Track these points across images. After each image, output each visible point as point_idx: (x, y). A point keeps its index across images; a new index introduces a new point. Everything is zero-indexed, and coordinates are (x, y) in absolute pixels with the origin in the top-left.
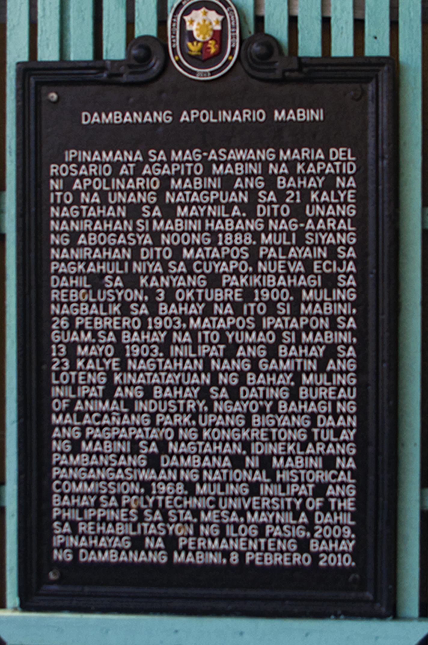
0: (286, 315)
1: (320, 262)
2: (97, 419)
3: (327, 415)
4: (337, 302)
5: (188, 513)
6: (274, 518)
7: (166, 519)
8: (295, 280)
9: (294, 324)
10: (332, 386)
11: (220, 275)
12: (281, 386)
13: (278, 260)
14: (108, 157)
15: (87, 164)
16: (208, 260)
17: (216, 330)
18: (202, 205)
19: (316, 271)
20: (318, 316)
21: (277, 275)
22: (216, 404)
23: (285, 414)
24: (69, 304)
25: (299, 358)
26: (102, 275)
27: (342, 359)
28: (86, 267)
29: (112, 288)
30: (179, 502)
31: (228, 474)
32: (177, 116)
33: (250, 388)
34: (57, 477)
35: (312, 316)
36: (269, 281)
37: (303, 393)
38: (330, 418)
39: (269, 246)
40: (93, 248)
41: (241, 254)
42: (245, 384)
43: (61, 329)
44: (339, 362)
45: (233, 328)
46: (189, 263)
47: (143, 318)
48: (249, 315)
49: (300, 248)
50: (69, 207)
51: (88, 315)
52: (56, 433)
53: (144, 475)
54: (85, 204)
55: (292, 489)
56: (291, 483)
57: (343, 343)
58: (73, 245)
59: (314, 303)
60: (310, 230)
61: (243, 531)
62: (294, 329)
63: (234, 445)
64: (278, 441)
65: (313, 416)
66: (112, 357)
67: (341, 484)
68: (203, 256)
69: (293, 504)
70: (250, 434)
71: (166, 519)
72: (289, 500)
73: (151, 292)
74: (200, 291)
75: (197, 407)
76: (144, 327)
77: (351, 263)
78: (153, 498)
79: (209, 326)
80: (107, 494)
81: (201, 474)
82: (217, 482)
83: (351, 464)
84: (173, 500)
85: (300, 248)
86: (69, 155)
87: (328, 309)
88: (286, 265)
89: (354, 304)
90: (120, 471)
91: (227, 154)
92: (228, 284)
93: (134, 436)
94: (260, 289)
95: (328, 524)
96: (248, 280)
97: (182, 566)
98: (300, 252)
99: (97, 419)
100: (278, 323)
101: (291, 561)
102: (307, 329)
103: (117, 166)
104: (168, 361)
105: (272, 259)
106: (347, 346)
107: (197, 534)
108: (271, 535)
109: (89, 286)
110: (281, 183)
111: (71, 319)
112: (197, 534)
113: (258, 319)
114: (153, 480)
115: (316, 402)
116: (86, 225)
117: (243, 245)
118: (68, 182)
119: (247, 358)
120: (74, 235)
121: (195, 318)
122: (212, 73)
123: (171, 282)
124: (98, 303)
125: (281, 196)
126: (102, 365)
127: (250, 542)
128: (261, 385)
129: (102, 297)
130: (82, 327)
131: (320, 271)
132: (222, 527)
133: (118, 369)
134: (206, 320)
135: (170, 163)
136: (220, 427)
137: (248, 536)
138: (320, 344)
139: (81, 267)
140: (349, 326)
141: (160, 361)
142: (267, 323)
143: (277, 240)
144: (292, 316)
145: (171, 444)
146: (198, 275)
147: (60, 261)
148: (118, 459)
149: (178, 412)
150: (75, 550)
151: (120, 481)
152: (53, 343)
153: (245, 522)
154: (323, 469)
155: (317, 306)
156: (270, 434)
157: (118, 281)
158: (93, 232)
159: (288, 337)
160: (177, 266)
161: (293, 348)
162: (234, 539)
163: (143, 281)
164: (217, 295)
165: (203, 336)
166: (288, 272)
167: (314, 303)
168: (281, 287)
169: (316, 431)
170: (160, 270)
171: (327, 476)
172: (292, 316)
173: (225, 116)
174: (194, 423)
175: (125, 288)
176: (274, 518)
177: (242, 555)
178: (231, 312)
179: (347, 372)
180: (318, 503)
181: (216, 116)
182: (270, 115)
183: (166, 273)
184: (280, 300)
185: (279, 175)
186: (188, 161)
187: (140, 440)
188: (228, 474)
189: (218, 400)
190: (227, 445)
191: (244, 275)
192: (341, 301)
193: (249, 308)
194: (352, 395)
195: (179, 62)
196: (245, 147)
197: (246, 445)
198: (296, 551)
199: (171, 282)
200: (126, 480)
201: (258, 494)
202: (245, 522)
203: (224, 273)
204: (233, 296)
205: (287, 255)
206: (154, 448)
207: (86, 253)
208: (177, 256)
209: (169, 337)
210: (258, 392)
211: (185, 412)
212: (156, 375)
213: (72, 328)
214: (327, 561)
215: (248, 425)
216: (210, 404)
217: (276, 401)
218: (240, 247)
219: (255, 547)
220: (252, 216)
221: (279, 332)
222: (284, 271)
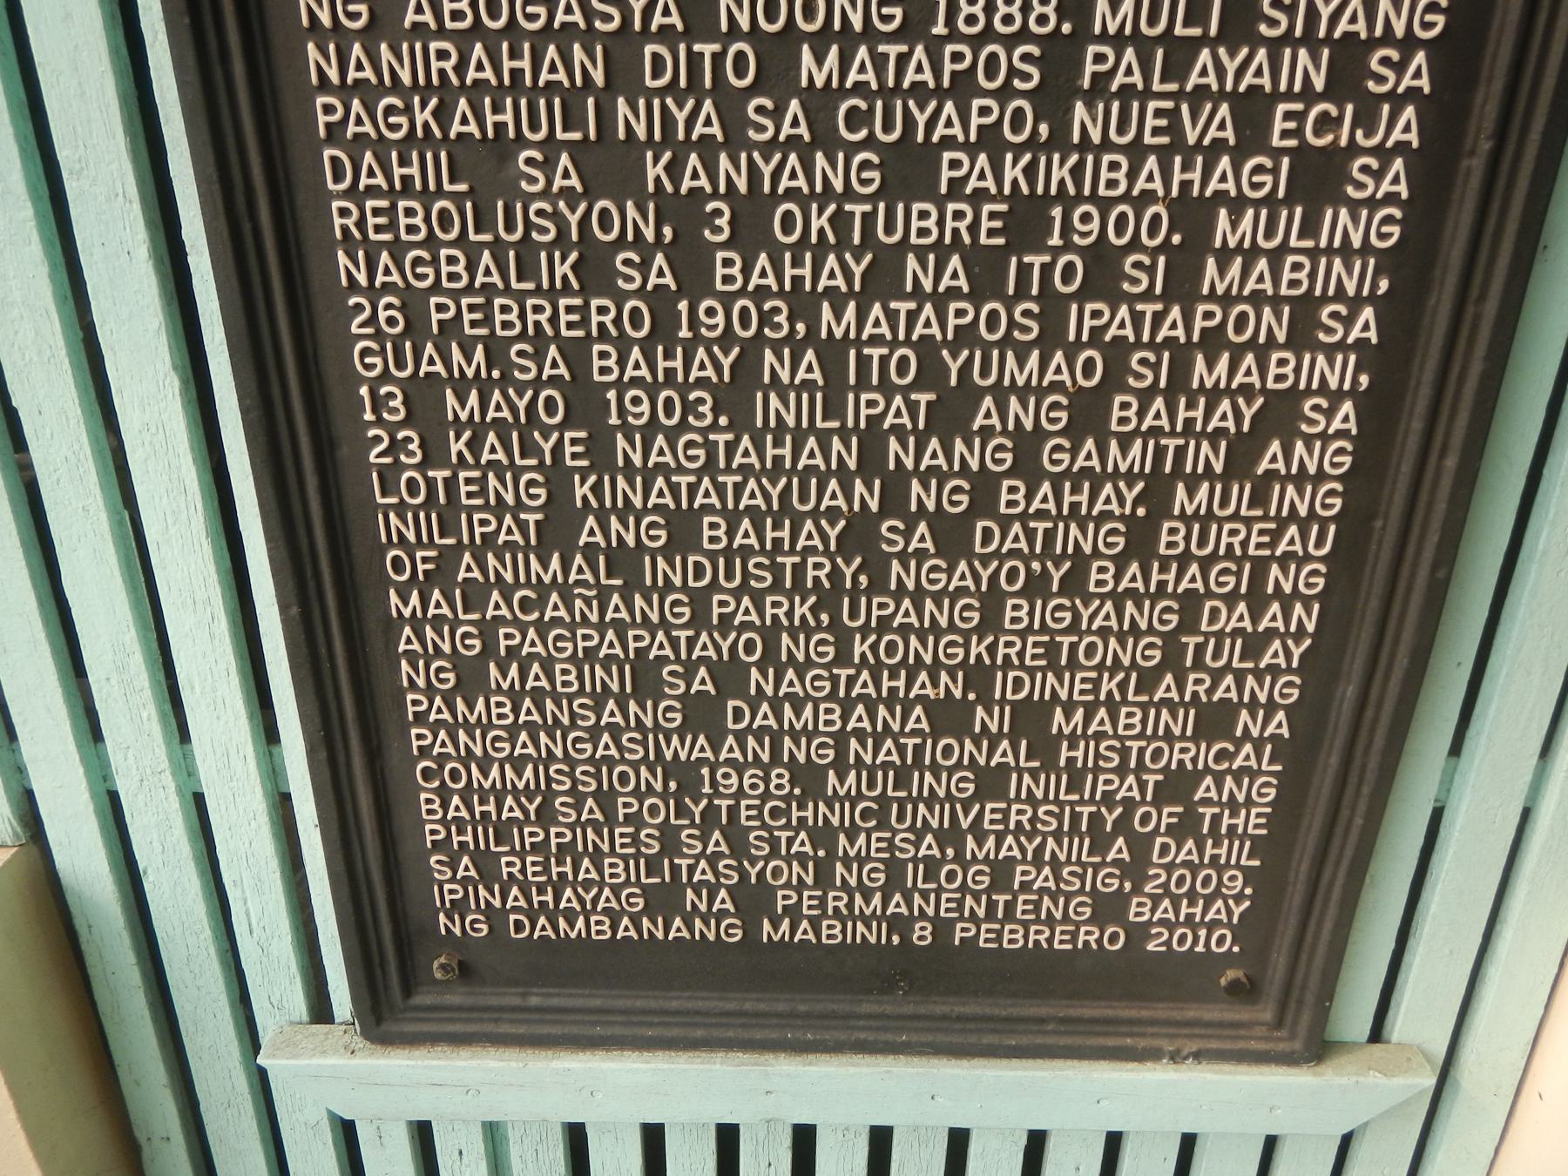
0: (1148, 296)
1: (1299, 107)
2: (525, 604)
3: (1231, 599)
4: (1329, 251)
5: (803, 835)
6: (1039, 850)
7: (738, 846)
8: (1196, 176)
9: (1173, 326)
10: (1265, 518)
11: (932, 152)
12: (1106, 516)
13: (1147, 94)
16: (888, 94)
17: (908, 342)
19: (1276, 142)
20: (1257, 298)
21: (1136, 151)
22: (896, 566)
23: (1103, 597)
24: (397, 249)
25: (1173, 434)
26: (502, 146)
27: (1309, 440)
28: (443, 114)
29: (545, 194)
30: (775, 813)
31: (918, 750)
33: (1005, 523)
34: (424, 752)
35: (1240, 298)
36: (1105, 175)
37: (1171, 537)
38: (1242, 607)
39: (1118, 41)
40: (464, 40)
41: (1012, 72)
42: (993, 514)
43: (379, 335)
44: (1299, 447)
45: (966, 336)
46: (820, 102)
47: (660, 300)
48: (1022, 292)
49: (1232, 54)
51: (469, 289)
52: (406, 640)
56: (1097, 770)
57: (1324, 388)
59: (1254, 252)
61: (951, 876)
62: (1170, 342)
63: (944, 677)
64: (1073, 664)
65: (1190, 604)
66: (562, 427)
67: (1238, 775)
68: (870, 76)
69: (1095, 818)
70: (992, 650)
71: (738, 846)
72: (1086, 810)
74: (859, 209)
75: (835, 575)
76: (663, 330)
77: (1409, 112)
78: (704, 802)
79: (885, 329)
80: (573, 791)
81: (841, 751)
82: (886, 766)
83: (1279, 724)
84: (760, 809)
85: (1232, 54)
87: (1294, 277)
88: (1174, 114)
89: (1389, 261)
90: (606, 738)
92: (956, 185)
94: (1070, 204)
95: (1186, 864)
96: (1030, 171)
98: (1231, 67)
99: (525, 604)
100: (1120, 323)
101: (1074, 940)
102: (1213, 342)
104: (746, 441)
105: (1126, 91)
106: (1337, 397)
107: (824, 878)
108: (1026, 887)
109: (462, 187)
111: (413, 304)
112: (824, 878)
113: (1052, 309)
114: (701, 762)
115: (1206, 564)
117: (1024, 35)
119: (1005, 432)
121: (838, 301)
123: (754, 174)
124: (497, 247)
127: (969, 901)
128: (1041, 515)
129: (510, 228)
130: (450, 328)
131: (1292, 143)
132: (894, 869)
133: (584, 463)
134: (877, 310)
136: (905, 630)
137: (963, 888)
138: (1247, 391)
140: (1355, 333)
141: (722, 438)
142: (1080, 320)
143: (1153, 21)
144: (1167, 297)
145: (754, 673)
147: (346, 90)
148: (598, 709)
151: (610, 762)
152: (362, 380)
153: (959, 857)
154: (1195, 738)
155: (1262, 264)
156: (1052, 649)
159: (1142, 370)
160: (777, 114)
161: (1159, 403)
162: (925, 895)
163: (654, 171)
164: (915, 224)
165: (864, 362)
166: (1178, 142)
167: (1254, 252)
168: (1148, 197)
170: (716, 130)
171: (1206, 755)
172: (1167, 297)
174: (825, 618)
175: (590, 194)
176: (1039, 850)
178: (963, 283)
179: (1321, 476)
180: (1170, 813)
183: (735, 141)
184: (1135, 245)
187: (662, 660)
188: (918, 750)
189: (903, 557)
190: (923, 676)
191: (1018, 150)
192: (1346, 251)
193: (1025, 270)
194: (1319, 543)
197: (978, 677)
198: (1085, 922)
199: (754, 174)
200: (623, 761)
201: (1002, 794)
202: (959, 857)
203: (948, 142)
204: (974, 228)
205: (1183, 79)
206: (703, 682)
209: (747, 366)
210: (1030, 535)
212: (706, 482)
213: (415, 327)
214: (1168, 943)
215: (990, 622)
216: (876, 568)
217: (1080, 562)
218: (1010, 42)
219: (981, 913)
221: (1117, 352)
222: (1165, 140)
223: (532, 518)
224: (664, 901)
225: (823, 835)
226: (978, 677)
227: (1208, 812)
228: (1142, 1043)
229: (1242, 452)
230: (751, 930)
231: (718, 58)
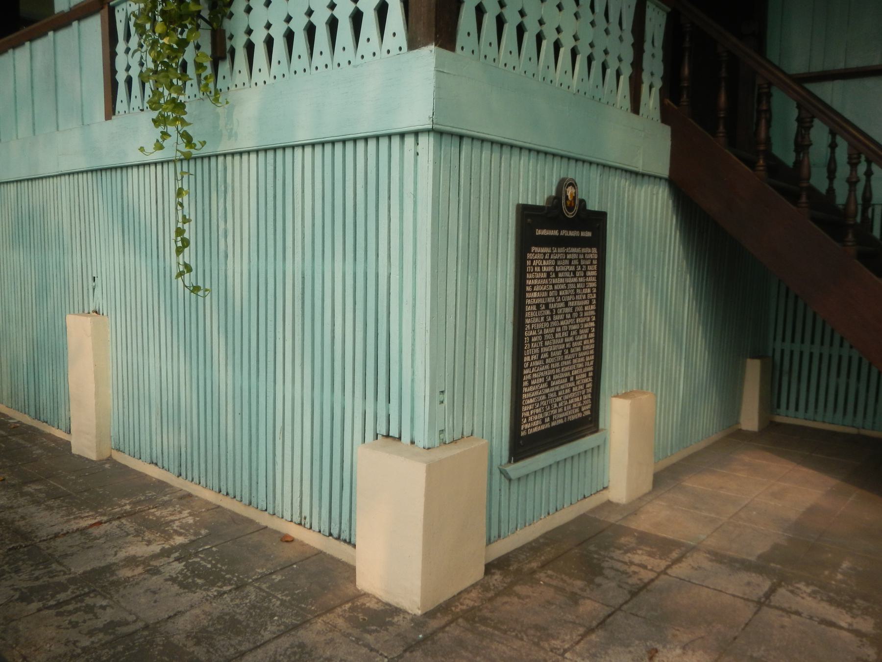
32: (559, 232)
37: (584, 348)
45: (571, 324)
46: (561, 296)
53: (547, 391)
58: (533, 291)
73: (551, 310)
86: (533, 249)
102: (586, 322)
103: (545, 254)
110: (583, 262)
116: (536, 282)
118: (532, 261)
120: (533, 286)
122: (573, 214)
125: (582, 267)
151: (541, 395)
157: (544, 308)
182: (580, 234)
197: (571, 371)
208: (558, 295)
216: (564, 358)
217: (578, 352)
220: (575, 276)
221: (580, 323)
225: (558, 403)
226: (571, 371)
230: (551, 424)
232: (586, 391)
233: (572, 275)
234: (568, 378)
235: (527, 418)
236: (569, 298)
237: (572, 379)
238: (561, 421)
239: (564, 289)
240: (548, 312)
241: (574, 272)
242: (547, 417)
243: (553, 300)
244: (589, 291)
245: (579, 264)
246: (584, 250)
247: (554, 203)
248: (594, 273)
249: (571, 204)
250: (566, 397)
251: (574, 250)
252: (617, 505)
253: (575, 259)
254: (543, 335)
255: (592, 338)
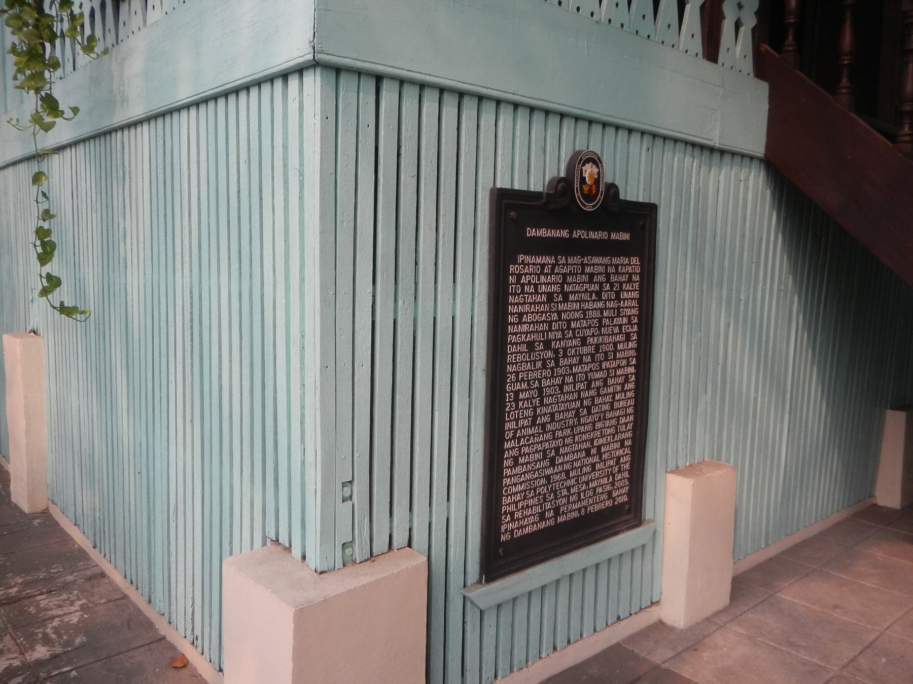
0: (611, 360)
14: (538, 261)
15: (529, 264)
18: (580, 292)
26: (534, 342)
32: (571, 233)
37: (616, 405)
39: (606, 318)
45: (591, 370)
46: (574, 330)
50: (519, 295)
53: (549, 472)
54: (527, 293)
55: (608, 463)
58: (520, 323)
60: (622, 307)
65: (618, 417)
66: (536, 398)
73: (556, 351)
74: (578, 348)
84: (559, 484)
86: (521, 258)
91: (591, 259)
93: (545, 447)
97: (561, 523)
102: (619, 367)
103: (543, 266)
110: (613, 279)
116: (526, 308)
118: (519, 276)
120: (521, 315)
122: (593, 206)
125: (612, 286)
126: (532, 403)
129: (533, 357)
135: (567, 265)
139: (523, 337)
146: (577, 338)
148: (536, 465)
149: (566, 428)
150: (512, 531)
151: (537, 478)
156: (601, 432)
157: (541, 347)
158: (530, 313)
163: (553, 344)
169: (618, 426)
171: (621, 451)
173: (593, 235)
175: (544, 350)
177: (586, 508)
181: (588, 236)
182: (610, 236)
183: (564, 339)
185: (612, 273)
186: (575, 264)
191: (596, 336)
195: (579, 197)
196: (598, 255)
197: (592, 441)
203: (589, 336)
207: (525, 328)
208: (569, 328)
211: (569, 427)
216: (579, 420)
217: (605, 412)
220: (600, 299)
221: (608, 370)
223: (530, 419)
224: (542, 517)
225: (568, 489)
226: (592, 441)
227: (622, 465)
228: (617, 529)
229: (623, 385)
230: (556, 520)
231: (562, 324)
232: (620, 468)
233: (594, 297)
234: (588, 452)
235: (512, 514)
236: (588, 332)
237: (594, 451)
238: (575, 515)
239: (580, 319)
240: (550, 354)
241: (599, 294)
242: (550, 509)
243: (559, 335)
244: (625, 320)
245: (608, 281)
246: (615, 261)
247: (559, 187)
248: (636, 295)
249: (590, 190)
250: (584, 479)
251: (597, 260)
252: (672, 629)
253: (601, 274)
254: (540, 389)
255: (630, 390)
